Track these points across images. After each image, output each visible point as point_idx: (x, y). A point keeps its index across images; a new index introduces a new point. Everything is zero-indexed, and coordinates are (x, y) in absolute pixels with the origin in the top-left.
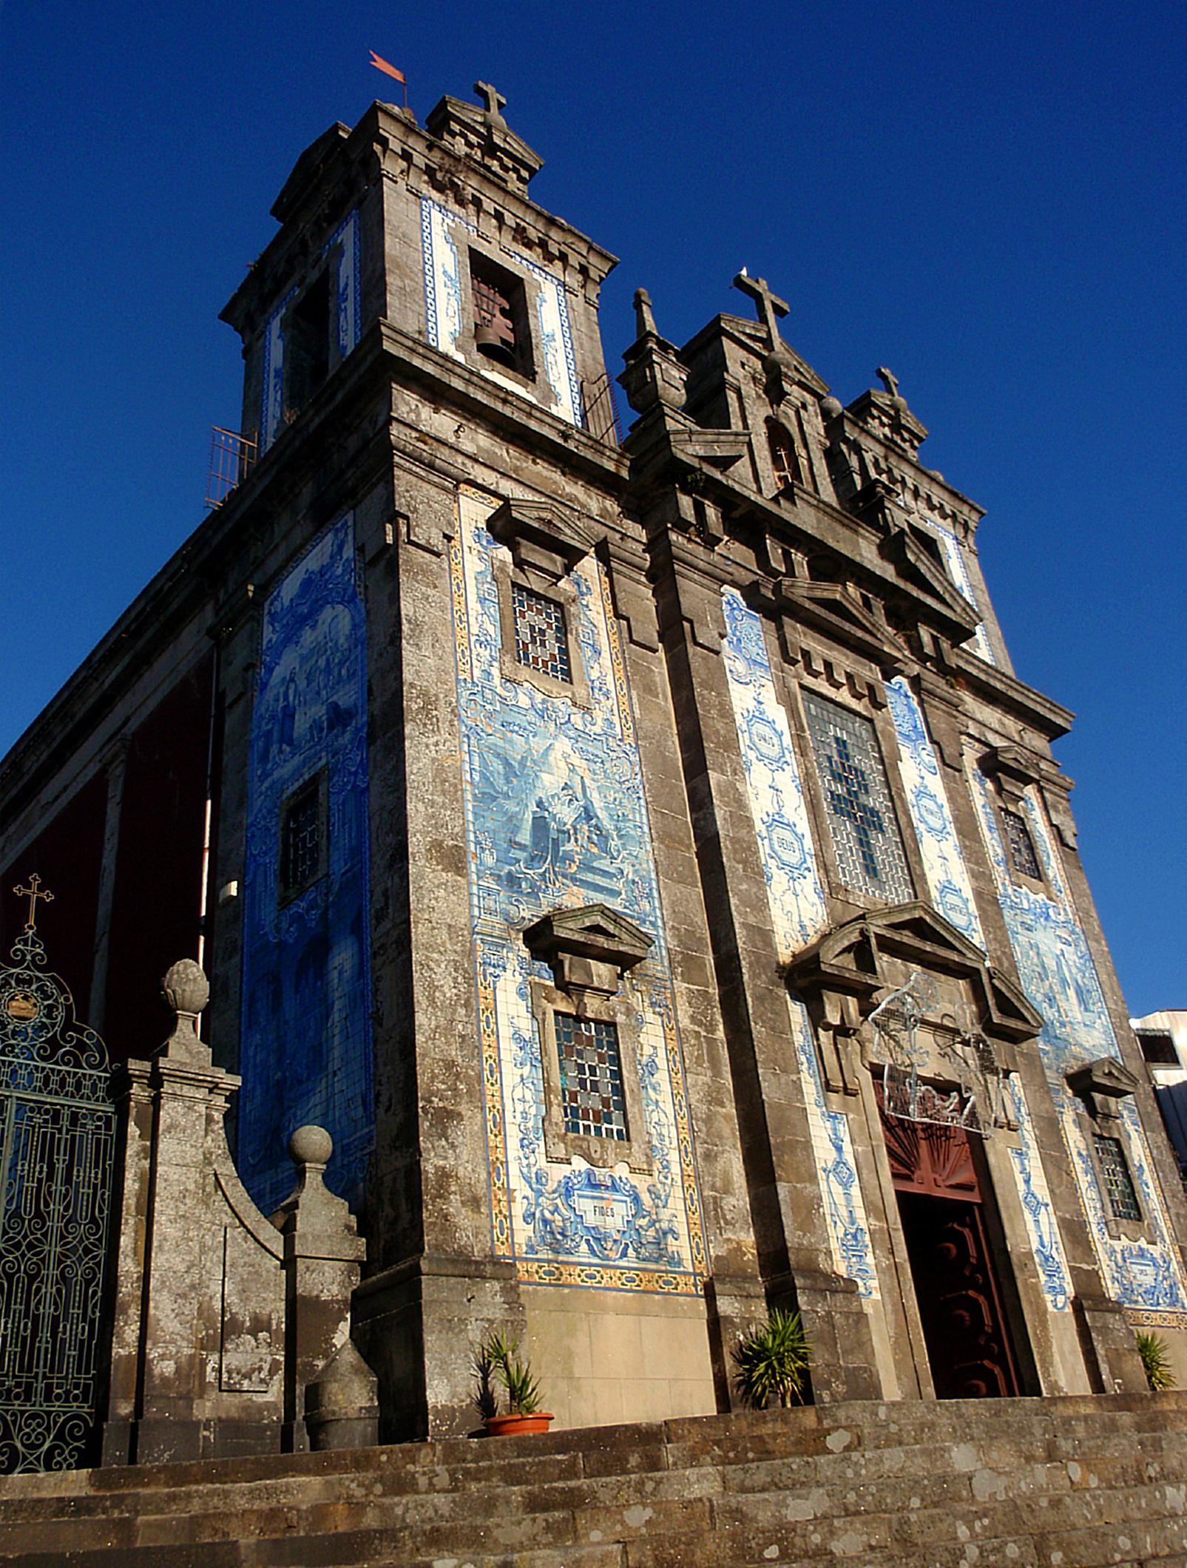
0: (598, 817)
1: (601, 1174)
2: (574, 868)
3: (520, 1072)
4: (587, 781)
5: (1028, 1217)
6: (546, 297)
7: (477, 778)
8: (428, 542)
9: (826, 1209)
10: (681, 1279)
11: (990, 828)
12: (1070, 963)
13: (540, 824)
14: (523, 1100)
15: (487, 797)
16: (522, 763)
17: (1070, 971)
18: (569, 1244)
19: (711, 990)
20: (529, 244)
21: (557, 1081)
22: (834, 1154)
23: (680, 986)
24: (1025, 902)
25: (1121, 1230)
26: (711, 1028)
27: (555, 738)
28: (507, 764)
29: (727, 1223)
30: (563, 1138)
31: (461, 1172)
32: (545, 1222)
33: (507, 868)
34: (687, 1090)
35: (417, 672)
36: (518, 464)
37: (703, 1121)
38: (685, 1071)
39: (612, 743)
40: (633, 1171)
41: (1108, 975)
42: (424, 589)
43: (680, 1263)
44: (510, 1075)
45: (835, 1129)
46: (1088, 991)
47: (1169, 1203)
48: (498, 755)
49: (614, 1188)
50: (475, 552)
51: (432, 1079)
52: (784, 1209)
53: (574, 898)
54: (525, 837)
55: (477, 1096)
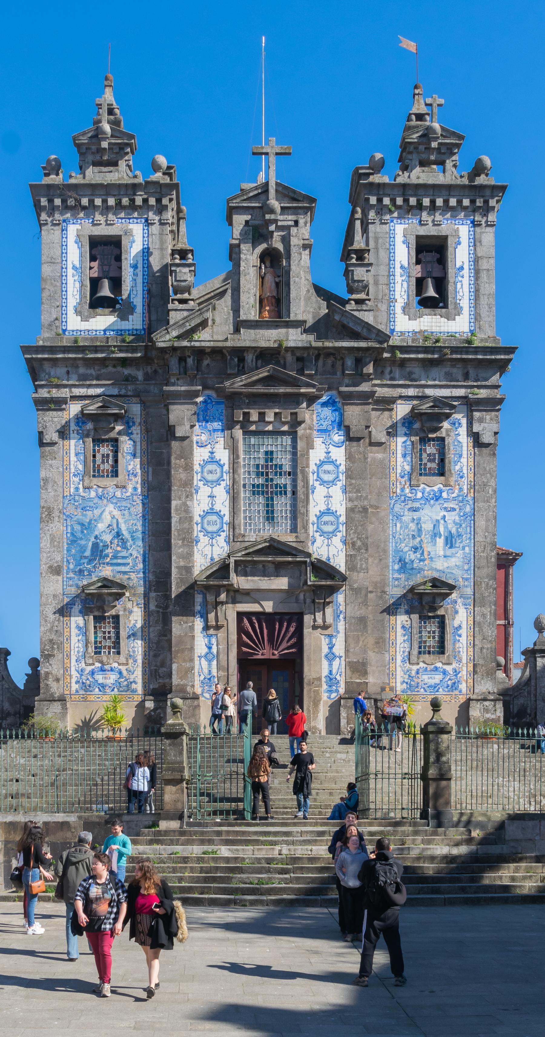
0: (123, 535)
1: (106, 667)
2: (109, 559)
3: (77, 638)
4: (119, 520)
5: (325, 663)
6: (135, 238)
7: (69, 535)
8: (51, 440)
9: (196, 670)
10: (136, 697)
11: (404, 456)
12: (449, 522)
13: (95, 546)
14: (78, 647)
15: (74, 541)
16: (90, 523)
17: (446, 527)
18: (91, 689)
19: (168, 593)
20: (124, 208)
21: (92, 638)
22: (206, 650)
23: (153, 594)
24: (419, 495)
25: (421, 660)
26: (167, 607)
27: (106, 506)
28: (82, 525)
29: (160, 677)
30: (92, 657)
31: (53, 672)
32: (83, 683)
33: (79, 568)
34: (149, 633)
35: (46, 501)
36: (99, 372)
37: (156, 643)
38: (150, 626)
39: (135, 498)
40: (119, 664)
41: (487, 520)
42: (50, 462)
43: (136, 691)
44: (74, 639)
45: (209, 641)
46: (460, 536)
47: (476, 643)
48: (79, 523)
49: (112, 670)
50: (75, 432)
51: (45, 645)
52: (174, 672)
53: (107, 572)
54: (88, 553)
55: (60, 647)
